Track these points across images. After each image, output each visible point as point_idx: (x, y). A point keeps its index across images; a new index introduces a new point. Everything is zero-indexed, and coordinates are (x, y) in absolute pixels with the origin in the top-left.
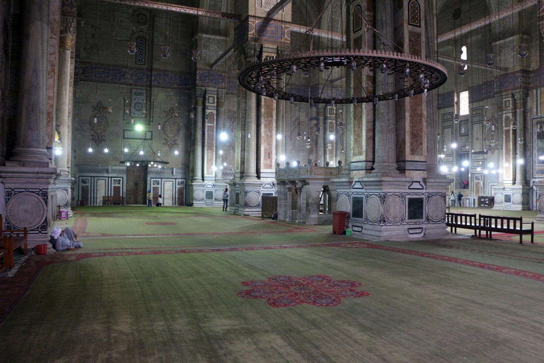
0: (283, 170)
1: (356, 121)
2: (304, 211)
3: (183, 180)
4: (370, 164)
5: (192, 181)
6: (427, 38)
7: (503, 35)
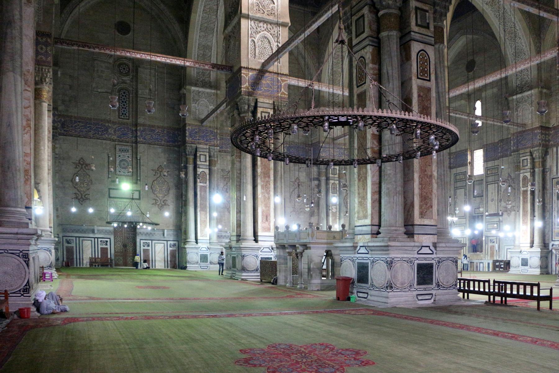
0: (282, 233)
1: (361, 183)
2: (305, 276)
3: (175, 242)
4: (376, 228)
5: (185, 244)
6: (438, 93)
7: (521, 89)
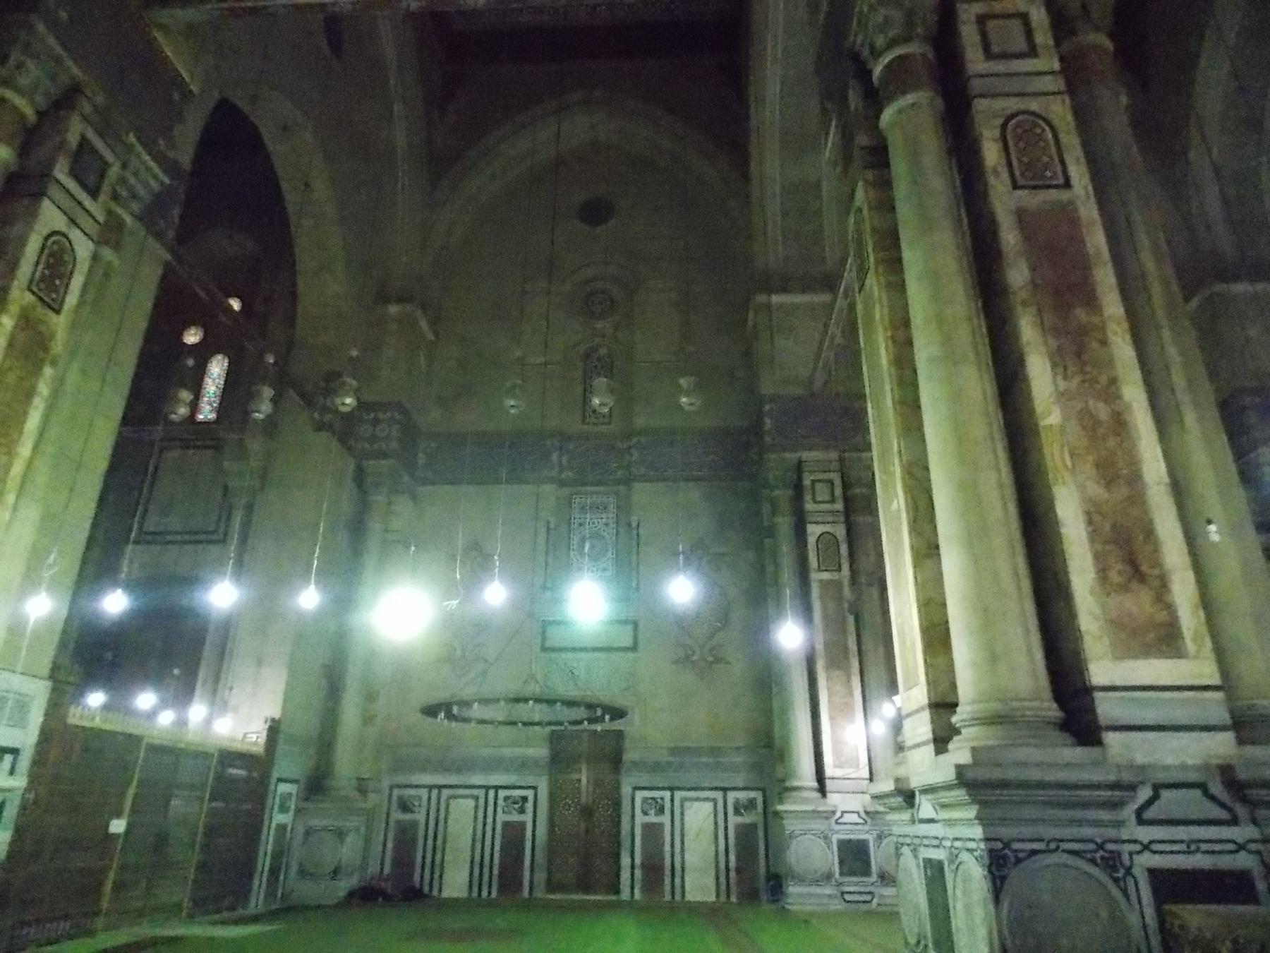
3: (752, 794)
